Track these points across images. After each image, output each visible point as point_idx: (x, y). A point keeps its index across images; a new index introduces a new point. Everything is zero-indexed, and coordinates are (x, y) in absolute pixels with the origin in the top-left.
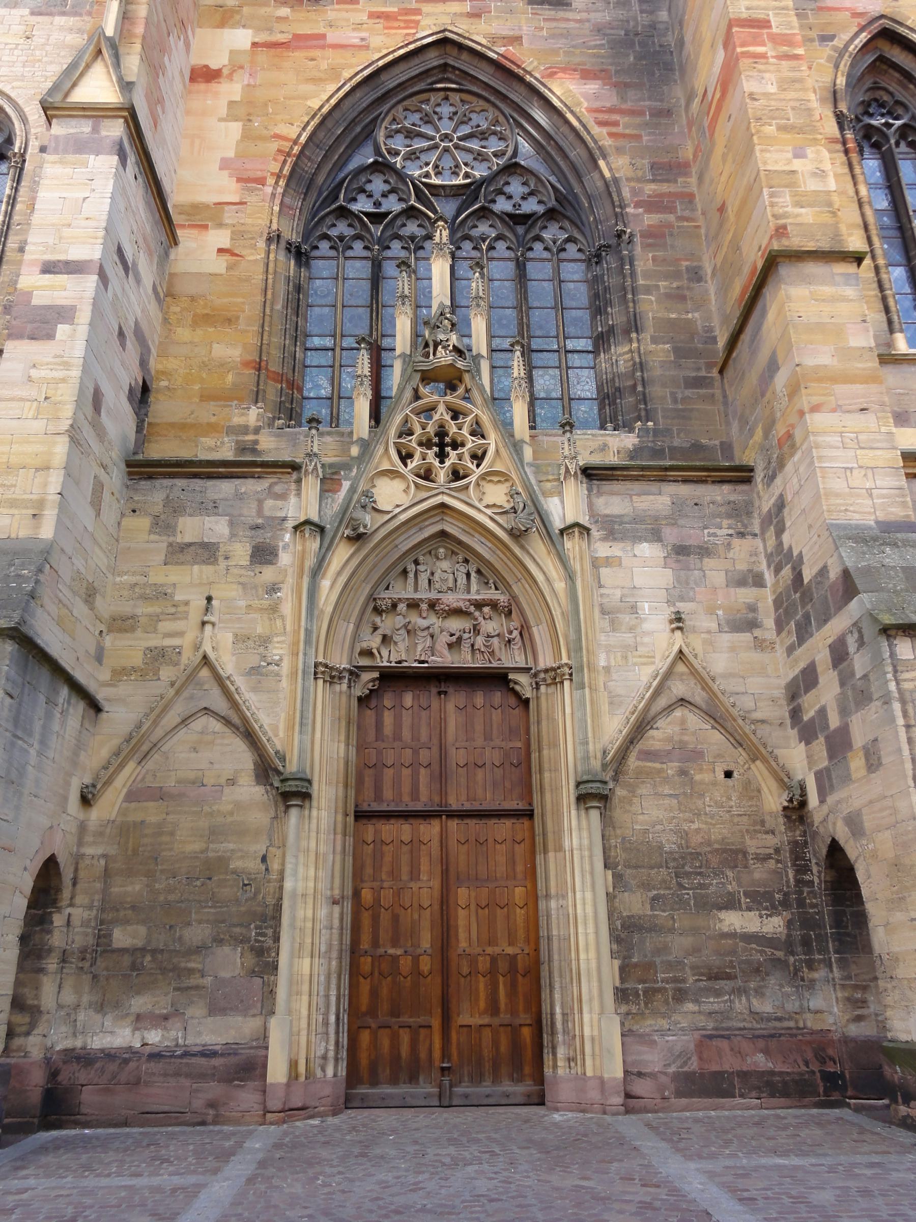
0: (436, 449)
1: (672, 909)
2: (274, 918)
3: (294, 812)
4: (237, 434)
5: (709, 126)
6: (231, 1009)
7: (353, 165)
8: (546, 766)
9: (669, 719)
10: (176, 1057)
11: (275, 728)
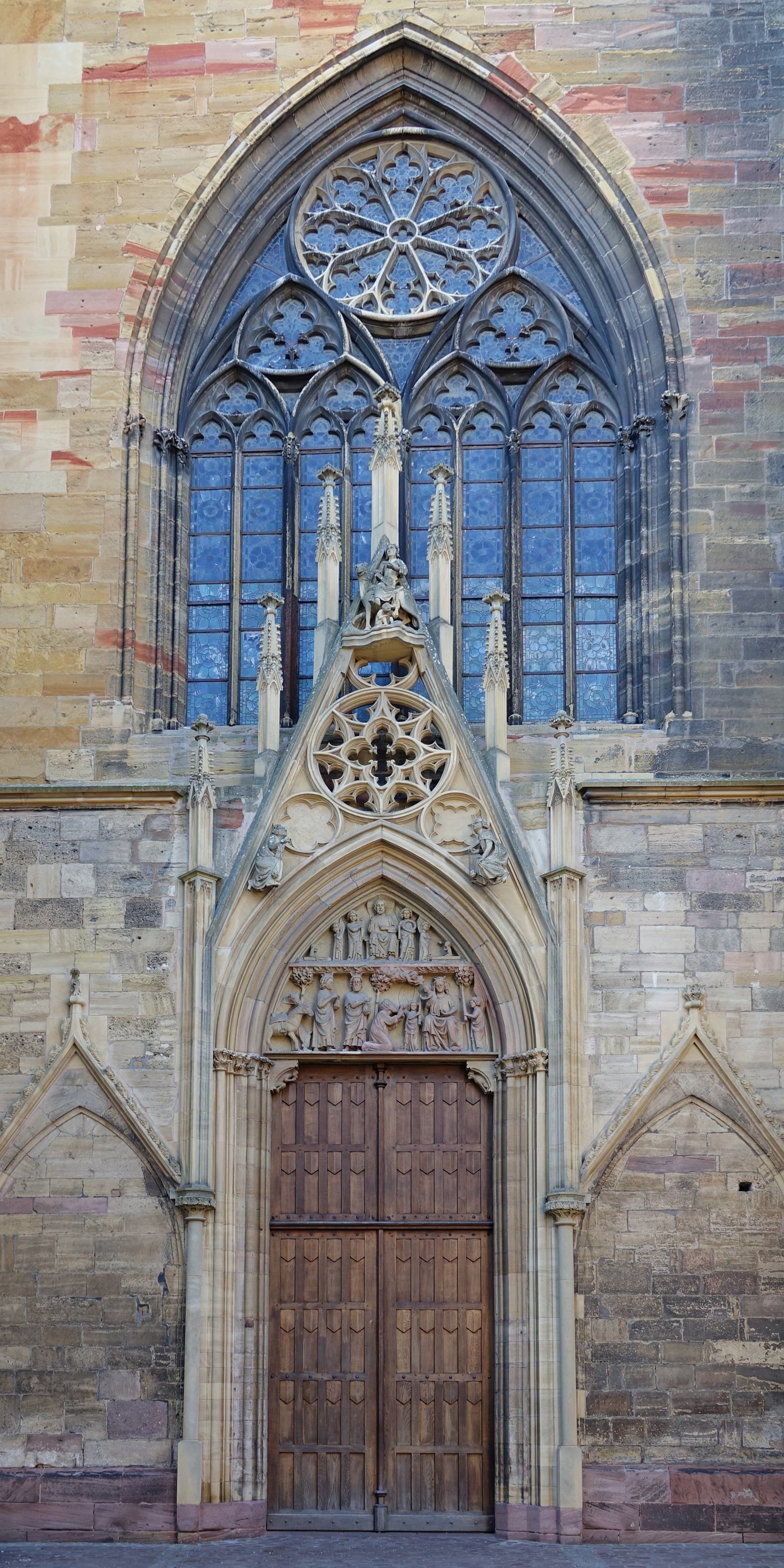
0: (374, 763)
3: (195, 1227)
6: (133, 1432)
8: (510, 1174)
9: (673, 1119)
11: (167, 1130)
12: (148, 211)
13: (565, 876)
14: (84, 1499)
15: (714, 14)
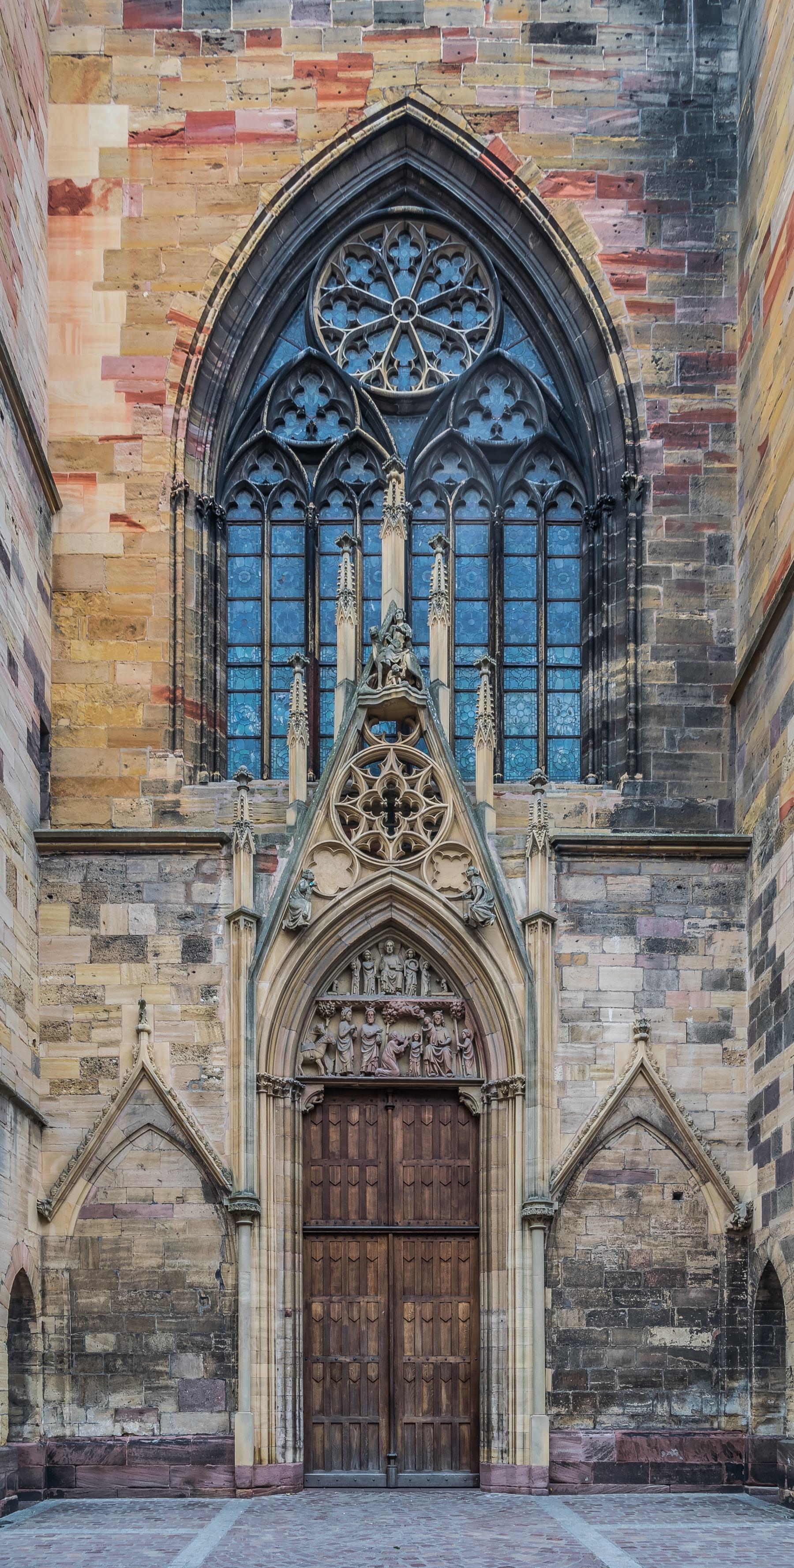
2: (231, 1328)
3: (245, 1231)
5: (766, 298)
6: (199, 1406)
7: (277, 363)
8: (493, 1186)
10: (154, 1444)
11: (220, 1146)
12: (188, 280)
13: (540, 921)
15: (671, 104)
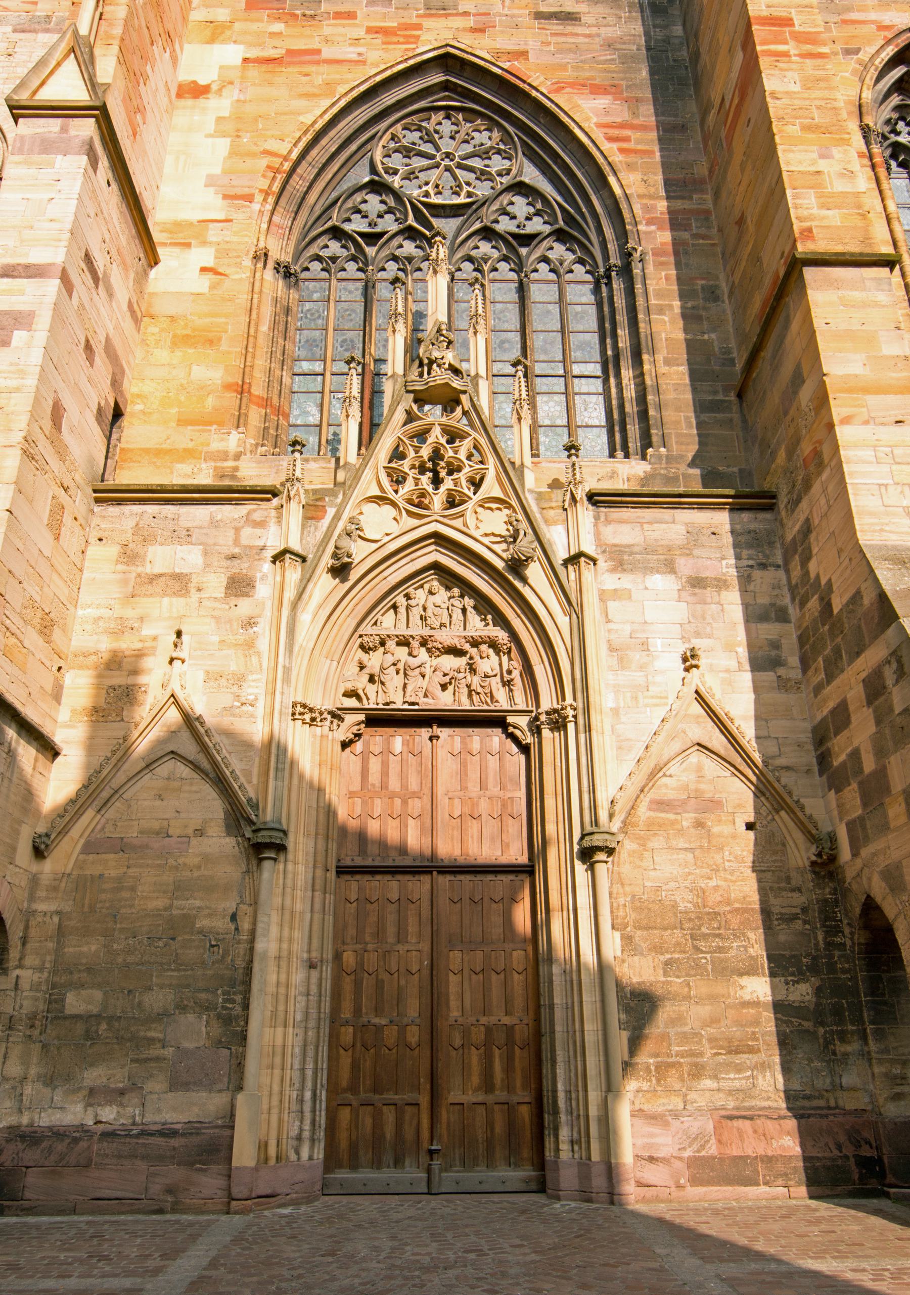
0: (430, 474)
1: (688, 975)
3: (267, 864)
4: (215, 460)
6: (195, 1083)
9: (684, 765)
11: (248, 774)
14: (138, 1162)
